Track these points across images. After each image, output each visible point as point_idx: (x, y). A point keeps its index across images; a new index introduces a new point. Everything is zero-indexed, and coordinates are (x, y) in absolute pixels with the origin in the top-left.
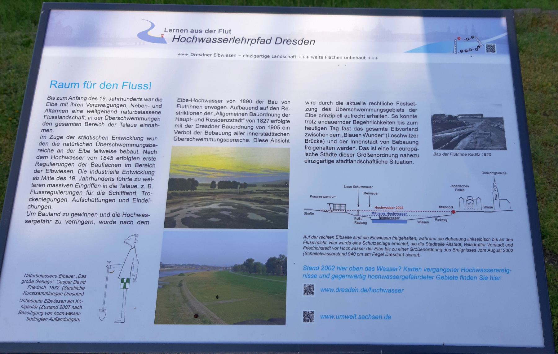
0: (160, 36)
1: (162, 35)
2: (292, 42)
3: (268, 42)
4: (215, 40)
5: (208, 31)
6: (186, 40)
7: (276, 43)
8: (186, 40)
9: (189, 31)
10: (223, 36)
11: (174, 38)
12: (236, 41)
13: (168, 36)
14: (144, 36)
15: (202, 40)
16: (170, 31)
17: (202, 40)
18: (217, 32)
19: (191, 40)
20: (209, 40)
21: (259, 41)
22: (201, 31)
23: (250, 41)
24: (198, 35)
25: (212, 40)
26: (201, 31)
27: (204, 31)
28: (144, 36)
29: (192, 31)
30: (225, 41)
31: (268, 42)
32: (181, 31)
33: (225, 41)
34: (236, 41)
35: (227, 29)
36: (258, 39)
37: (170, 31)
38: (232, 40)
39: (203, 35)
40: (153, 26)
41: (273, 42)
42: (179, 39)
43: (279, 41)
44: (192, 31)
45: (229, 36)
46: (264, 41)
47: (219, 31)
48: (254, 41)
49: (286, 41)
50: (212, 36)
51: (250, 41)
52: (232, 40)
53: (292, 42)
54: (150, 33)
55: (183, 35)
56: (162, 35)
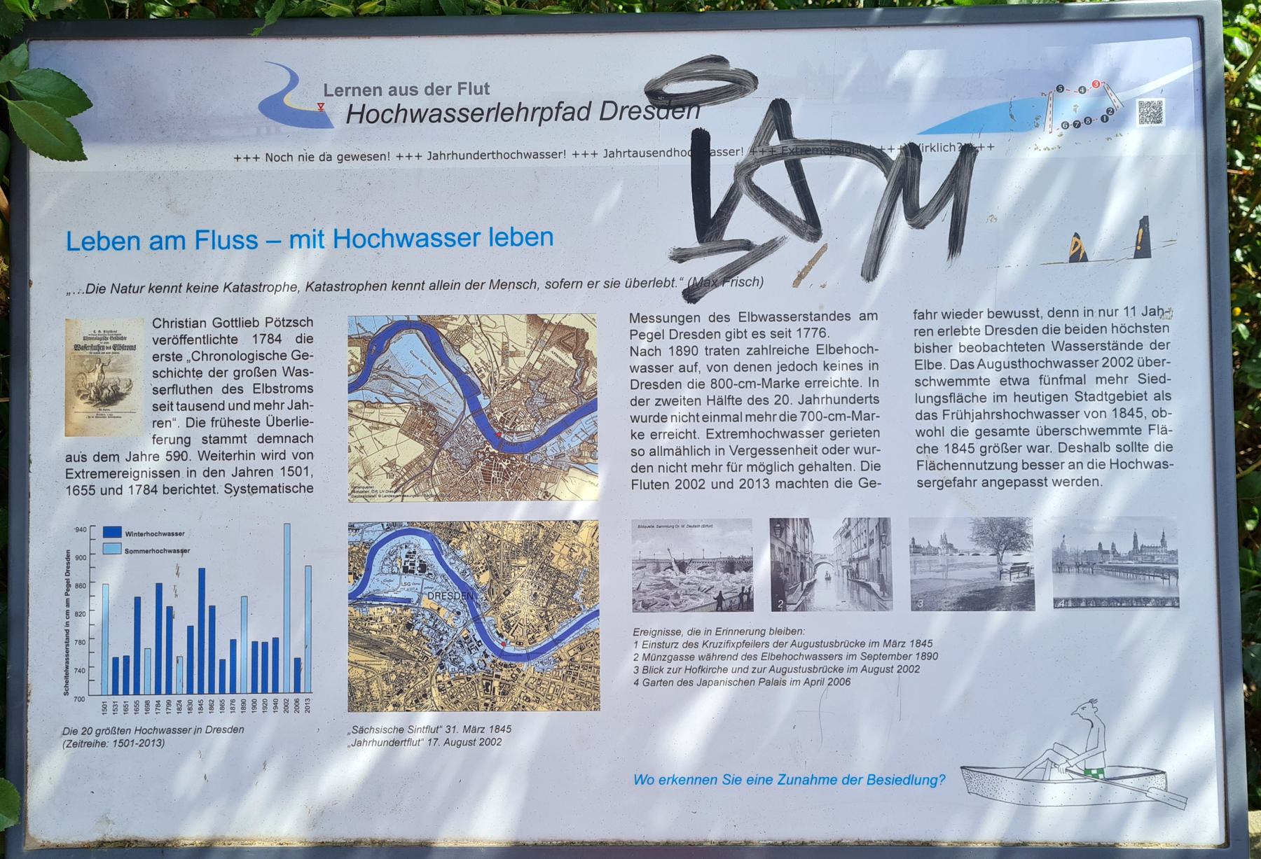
0: (316, 108)
1: (321, 105)
2: (644, 112)
3: (583, 114)
4: (450, 116)
5: (433, 90)
6: (380, 116)
7: (602, 119)
8: (380, 116)
9: (386, 91)
10: (469, 101)
11: (350, 113)
12: (504, 114)
13: (337, 109)
14: (274, 108)
15: (418, 116)
16: (339, 91)
17: (418, 116)
18: (455, 89)
19: (393, 116)
20: (437, 116)
21: (561, 112)
22: (414, 91)
23: (538, 112)
24: (409, 103)
25: (444, 115)
26: (414, 91)
27: (421, 90)
28: (274, 108)
29: (393, 91)
30: (475, 115)
31: (583, 114)
32: (366, 91)
33: (475, 115)
34: (504, 114)
35: (478, 83)
36: (558, 108)
37: (339, 91)
38: (493, 113)
39: (420, 102)
40: (294, 80)
41: (595, 114)
42: (362, 114)
43: (609, 111)
44: (393, 91)
45: (485, 102)
46: (572, 114)
47: (460, 89)
48: (546, 115)
49: (626, 111)
50: (442, 102)
51: (538, 112)
52: (493, 113)
53: (644, 112)
54: (290, 100)
55: (373, 102)
56: (321, 105)
